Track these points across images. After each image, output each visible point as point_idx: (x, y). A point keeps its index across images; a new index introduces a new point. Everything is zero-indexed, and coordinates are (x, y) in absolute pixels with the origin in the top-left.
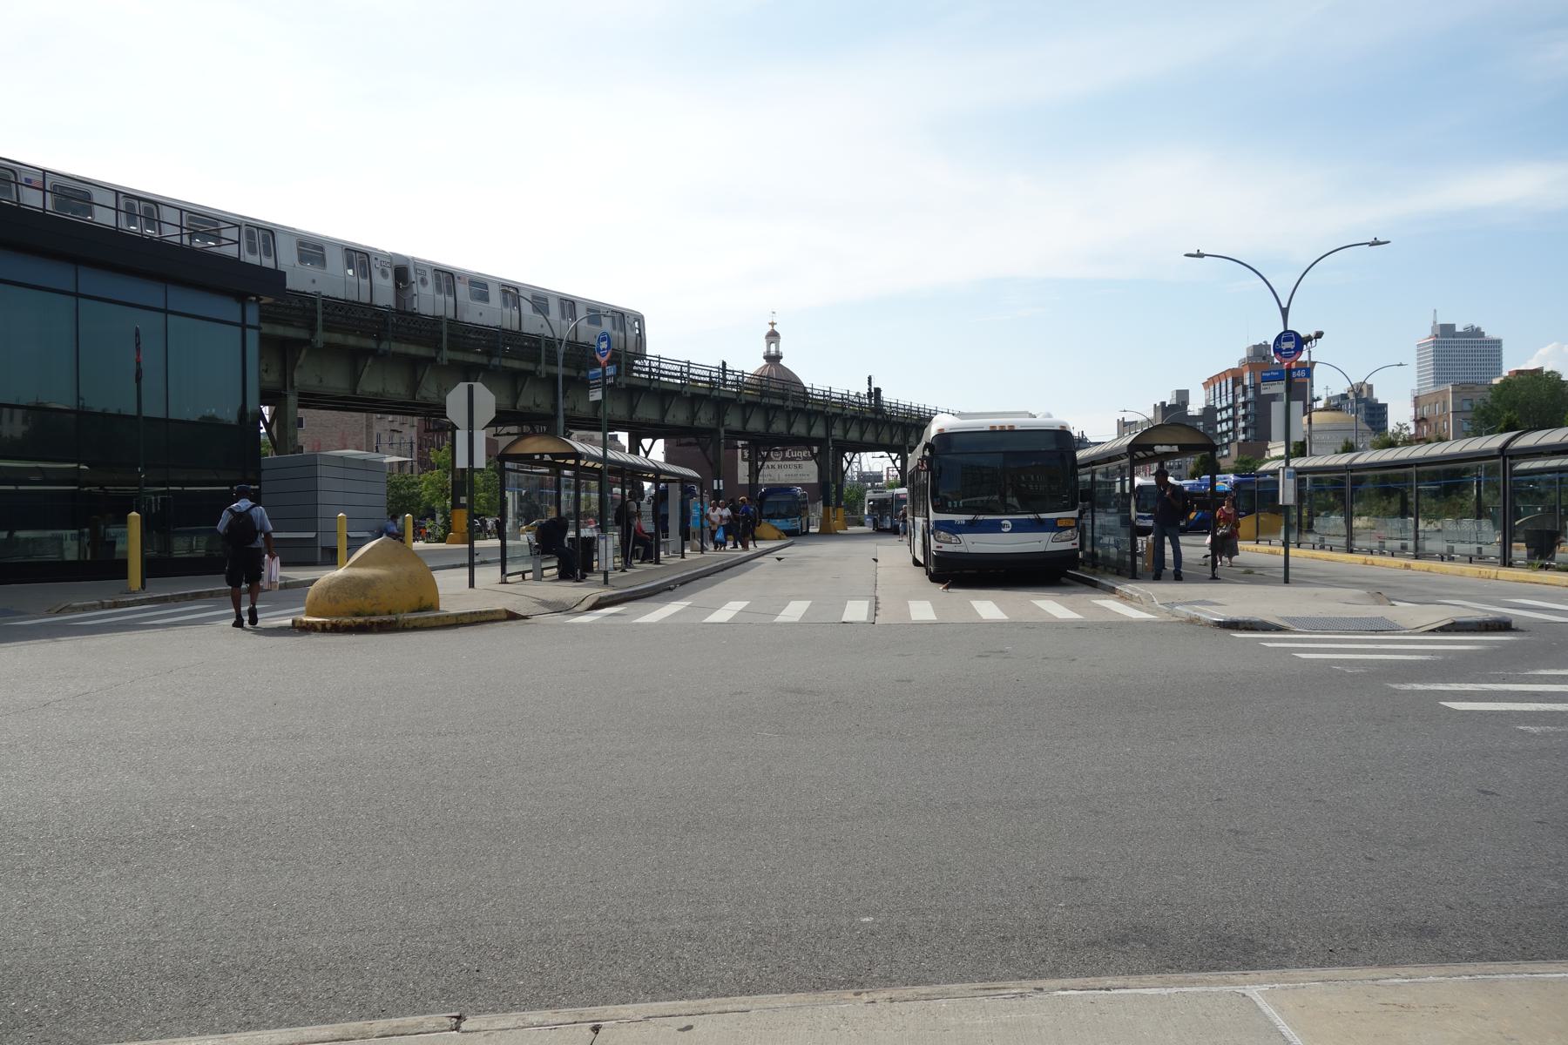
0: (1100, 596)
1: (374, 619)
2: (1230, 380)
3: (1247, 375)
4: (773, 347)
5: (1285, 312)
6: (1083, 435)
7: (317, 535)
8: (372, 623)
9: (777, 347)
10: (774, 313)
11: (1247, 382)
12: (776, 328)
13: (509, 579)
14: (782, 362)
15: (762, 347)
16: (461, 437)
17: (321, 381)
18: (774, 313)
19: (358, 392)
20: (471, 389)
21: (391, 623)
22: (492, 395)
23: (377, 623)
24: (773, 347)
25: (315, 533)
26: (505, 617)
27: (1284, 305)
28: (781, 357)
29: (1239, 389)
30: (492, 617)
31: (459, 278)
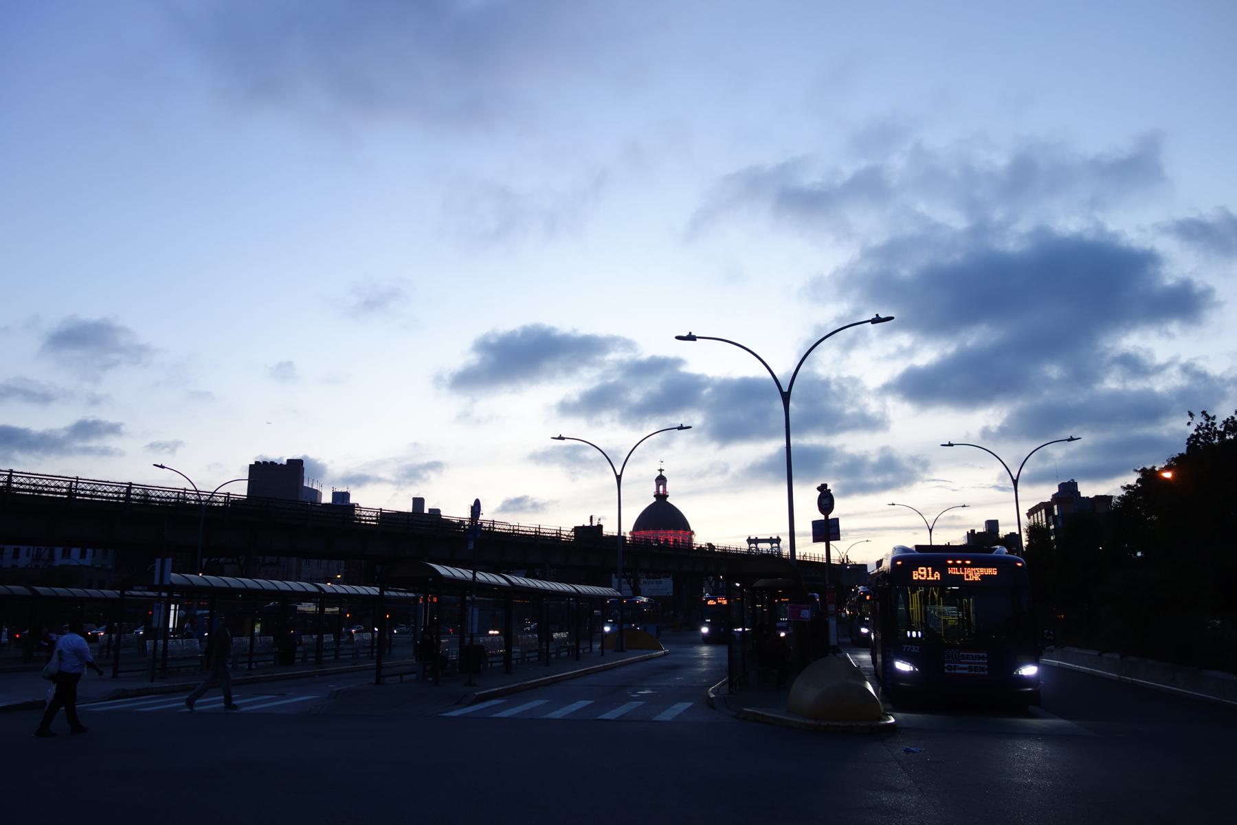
2: (1043, 511)
3: (1055, 507)
4: (661, 487)
5: (619, 478)
6: (847, 559)
9: (665, 488)
10: (662, 462)
11: (1056, 513)
12: (663, 473)
14: (668, 500)
15: (652, 488)
18: (662, 462)
24: (661, 487)
27: (619, 473)
28: (668, 496)
29: (1051, 518)
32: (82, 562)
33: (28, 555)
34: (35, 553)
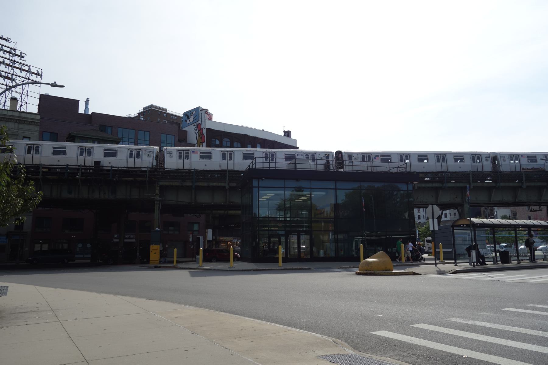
0: (500, 272)
1: (369, 272)
7: (452, 250)
8: (368, 273)
13: (457, 264)
16: (431, 221)
17: (477, 199)
19: (491, 201)
20: (432, 207)
21: (373, 273)
22: (438, 208)
23: (370, 273)
25: (451, 250)
26: (413, 274)
30: (407, 274)
31: (522, 156)
32: (445, 219)
33: (424, 218)
34: (426, 217)
